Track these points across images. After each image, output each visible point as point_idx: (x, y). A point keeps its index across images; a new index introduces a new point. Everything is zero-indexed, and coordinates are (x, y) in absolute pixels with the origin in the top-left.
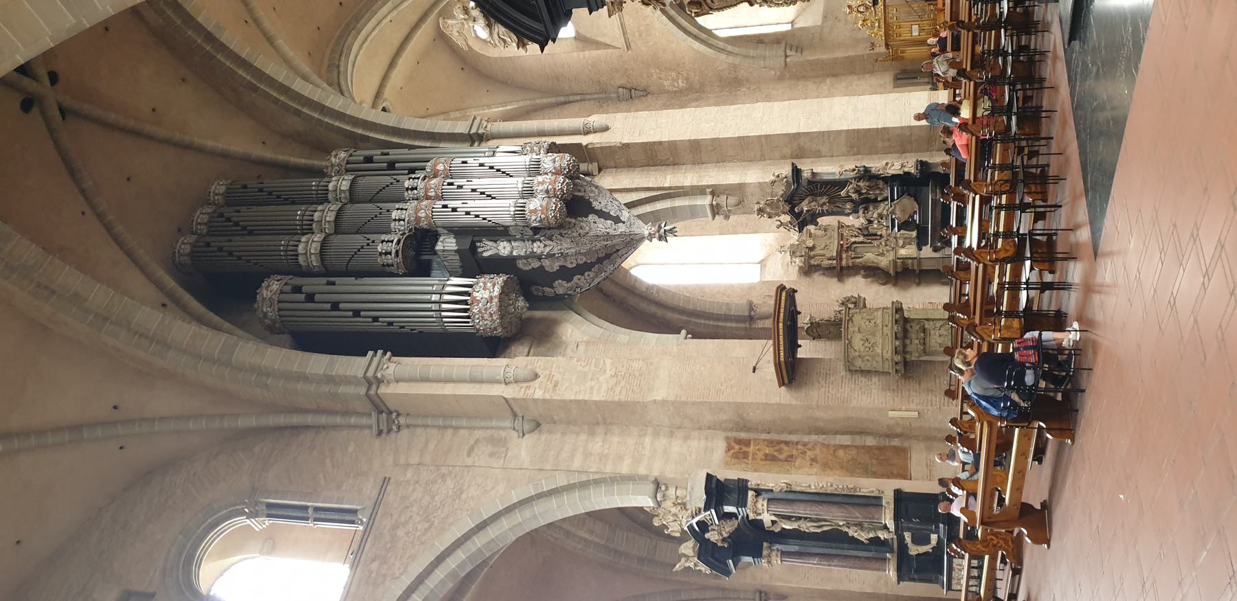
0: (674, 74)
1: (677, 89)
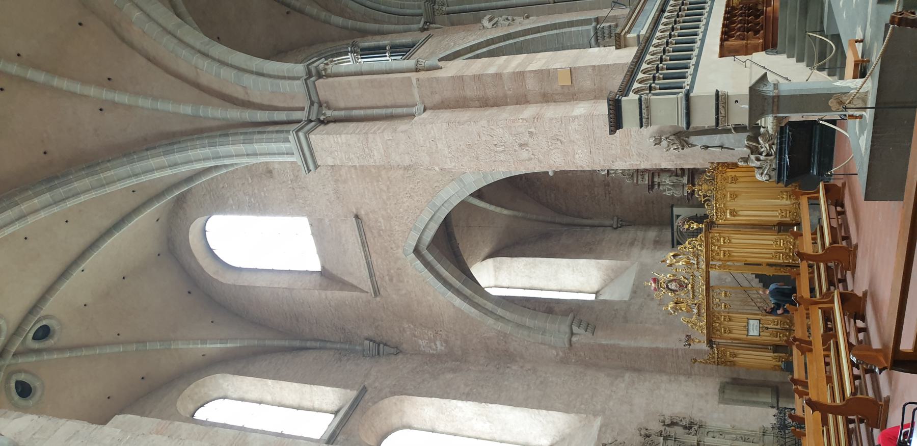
0: (430, 334)
1: (435, 352)
